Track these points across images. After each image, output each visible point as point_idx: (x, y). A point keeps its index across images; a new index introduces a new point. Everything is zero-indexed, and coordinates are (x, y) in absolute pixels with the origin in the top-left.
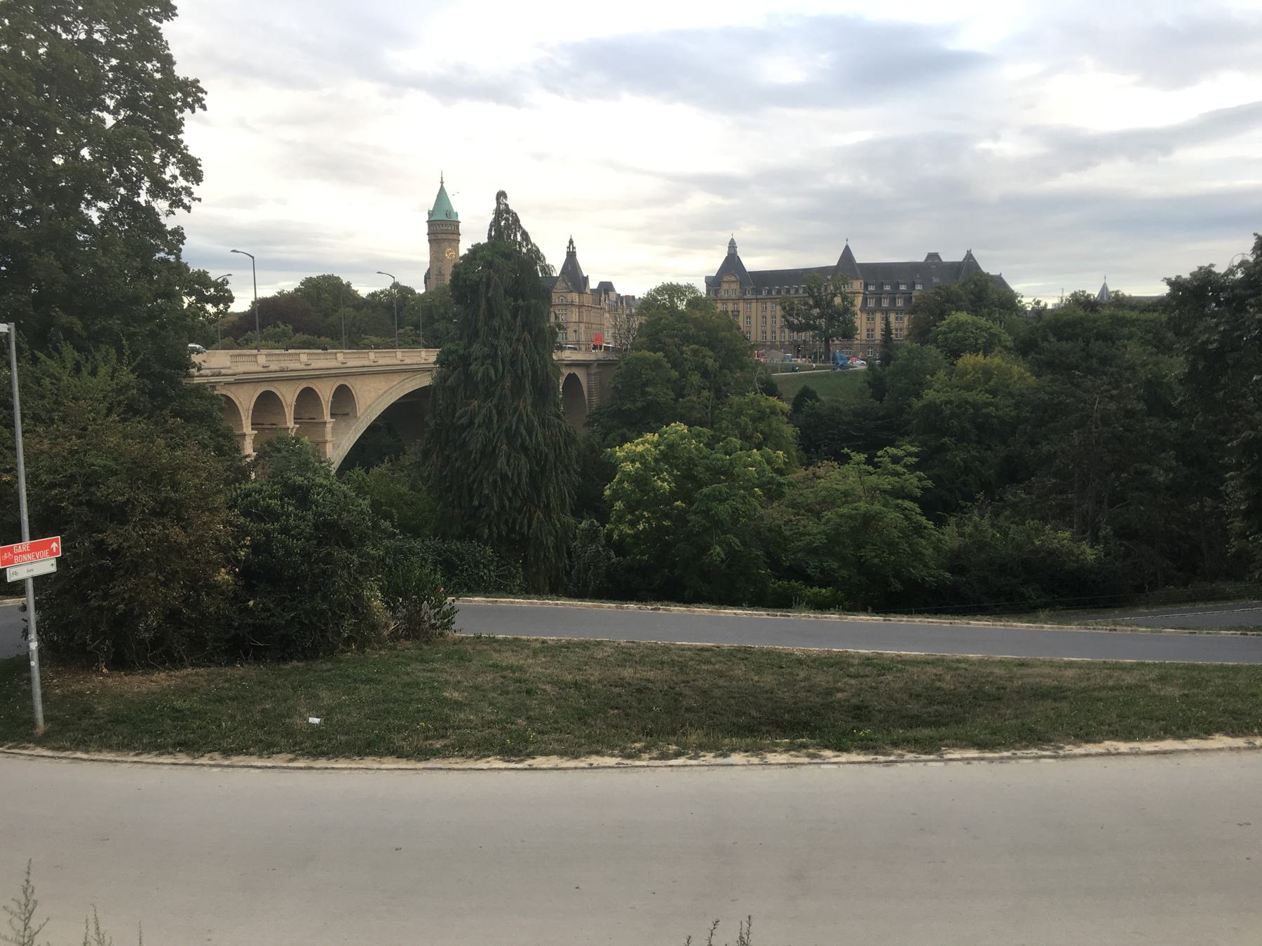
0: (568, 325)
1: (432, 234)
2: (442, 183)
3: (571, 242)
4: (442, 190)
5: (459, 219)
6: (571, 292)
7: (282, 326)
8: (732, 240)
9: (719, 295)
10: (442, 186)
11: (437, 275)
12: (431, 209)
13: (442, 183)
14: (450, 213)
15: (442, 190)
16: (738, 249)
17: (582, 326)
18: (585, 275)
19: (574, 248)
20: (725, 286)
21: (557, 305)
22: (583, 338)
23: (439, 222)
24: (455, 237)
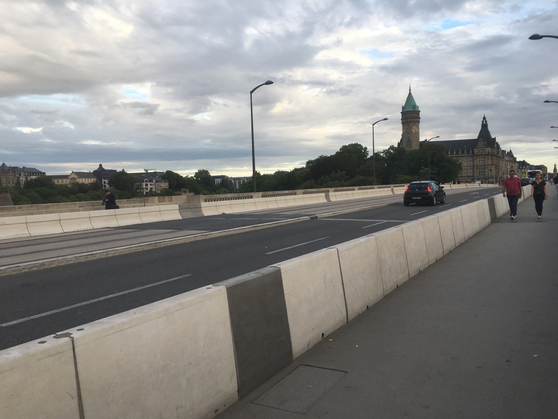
0: (486, 166)
1: (404, 119)
2: (410, 90)
3: (484, 118)
4: (410, 94)
5: (420, 109)
6: (488, 147)
7: (340, 172)
10: (410, 93)
12: (404, 105)
13: (410, 90)
14: (415, 106)
15: (410, 94)
19: (486, 122)
21: (478, 155)
23: (409, 112)
24: (418, 120)
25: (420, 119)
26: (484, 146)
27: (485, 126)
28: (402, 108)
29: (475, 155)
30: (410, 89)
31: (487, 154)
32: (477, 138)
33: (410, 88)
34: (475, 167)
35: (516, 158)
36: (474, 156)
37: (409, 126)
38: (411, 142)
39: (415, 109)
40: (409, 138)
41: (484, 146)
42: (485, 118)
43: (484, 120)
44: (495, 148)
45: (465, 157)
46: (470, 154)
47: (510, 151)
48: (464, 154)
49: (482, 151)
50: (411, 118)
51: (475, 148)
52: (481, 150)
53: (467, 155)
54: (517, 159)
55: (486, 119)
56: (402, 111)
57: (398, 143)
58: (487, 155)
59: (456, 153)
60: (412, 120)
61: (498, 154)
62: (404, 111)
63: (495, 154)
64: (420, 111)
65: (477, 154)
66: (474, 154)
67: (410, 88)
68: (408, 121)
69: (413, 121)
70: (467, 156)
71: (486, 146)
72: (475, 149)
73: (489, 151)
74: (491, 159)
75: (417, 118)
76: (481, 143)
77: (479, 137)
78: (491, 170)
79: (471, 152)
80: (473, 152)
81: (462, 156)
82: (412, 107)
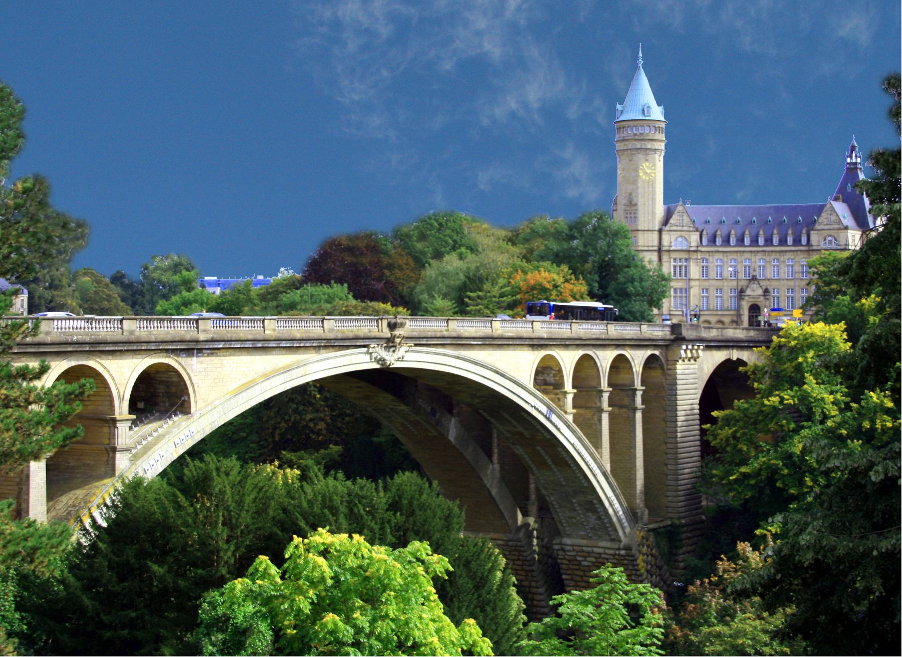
11: (625, 205)
31: (842, 247)
37: (630, 161)
38: (636, 205)
39: (649, 116)
45: (788, 255)
48: (771, 245)
49: (830, 238)
50: (636, 140)
51: (813, 230)
52: (830, 236)
59: (766, 241)
60: (639, 147)
66: (812, 246)
70: (794, 251)
71: (842, 227)
72: (812, 232)
73: (847, 241)
79: (804, 240)
81: (780, 252)
82: (641, 110)
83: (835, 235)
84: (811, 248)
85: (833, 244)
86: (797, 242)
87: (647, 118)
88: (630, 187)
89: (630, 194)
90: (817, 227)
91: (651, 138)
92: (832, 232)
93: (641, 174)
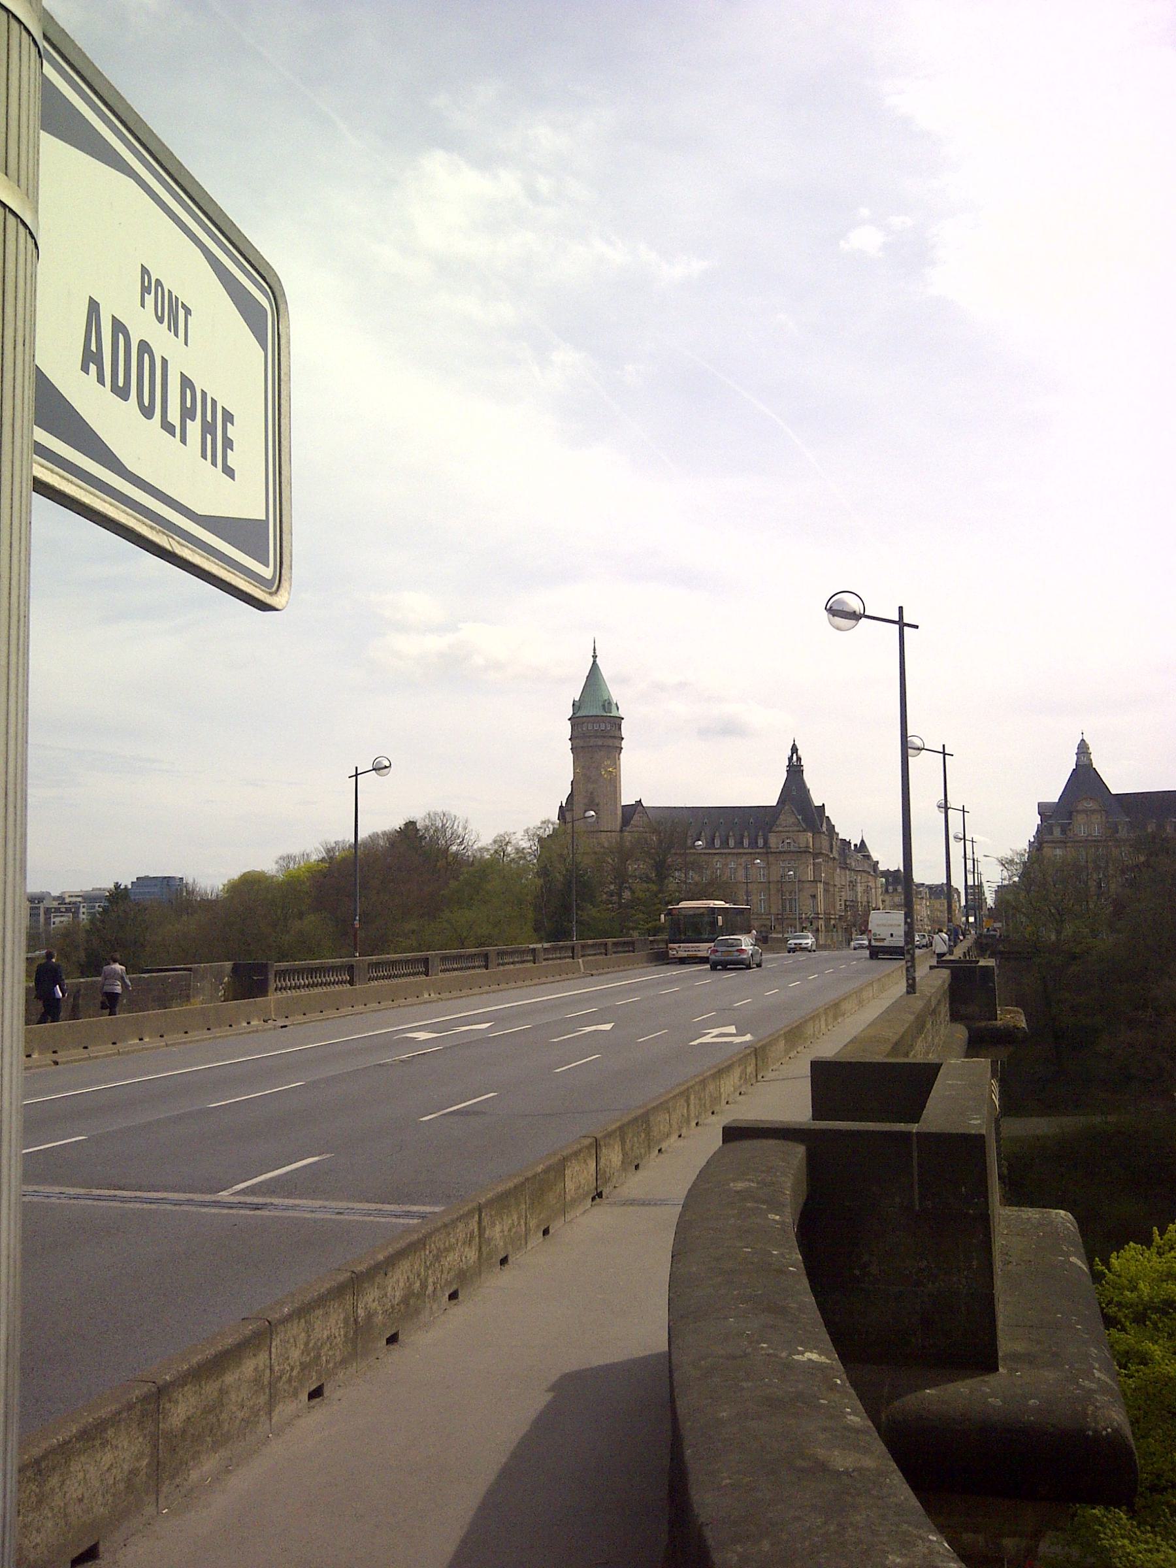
2: (595, 657)
3: (794, 749)
5: (621, 713)
8: (1083, 740)
9: (1070, 834)
10: (594, 662)
12: (577, 699)
13: (595, 657)
14: (608, 704)
16: (1092, 757)
17: (821, 886)
18: (817, 802)
19: (799, 759)
20: (1080, 819)
21: (780, 852)
22: (821, 908)
25: (623, 742)
26: (796, 828)
27: (795, 770)
28: (573, 705)
29: (771, 853)
30: (594, 653)
31: (802, 850)
32: (774, 804)
33: (594, 650)
34: (772, 886)
35: (877, 862)
36: (770, 855)
39: (611, 712)
40: (592, 793)
41: (796, 828)
42: (797, 750)
43: (795, 755)
44: (822, 836)
46: (758, 847)
47: (863, 841)
49: (788, 841)
53: (750, 851)
54: (879, 865)
55: (799, 752)
56: (574, 714)
57: (561, 807)
58: (805, 852)
59: (722, 843)
61: (831, 852)
62: (577, 715)
63: (824, 852)
64: (623, 719)
65: (778, 850)
66: (770, 848)
67: (594, 650)
68: (591, 744)
69: (603, 746)
72: (770, 834)
74: (814, 864)
75: (614, 737)
76: (787, 819)
77: (782, 799)
78: (814, 897)
79: (761, 842)
80: (766, 842)
83: (794, 837)
84: (769, 850)
85: (792, 846)
86: (754, 844)
87: (609, 714)
88: (591, 786)
89: (592, 793)
90: (774, 829)
91: (613, 735)
92: (791, 834)
93: (603, 773)
